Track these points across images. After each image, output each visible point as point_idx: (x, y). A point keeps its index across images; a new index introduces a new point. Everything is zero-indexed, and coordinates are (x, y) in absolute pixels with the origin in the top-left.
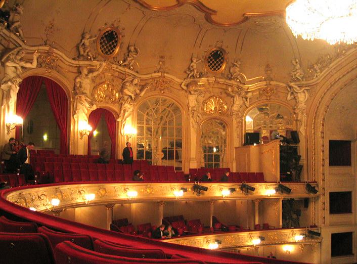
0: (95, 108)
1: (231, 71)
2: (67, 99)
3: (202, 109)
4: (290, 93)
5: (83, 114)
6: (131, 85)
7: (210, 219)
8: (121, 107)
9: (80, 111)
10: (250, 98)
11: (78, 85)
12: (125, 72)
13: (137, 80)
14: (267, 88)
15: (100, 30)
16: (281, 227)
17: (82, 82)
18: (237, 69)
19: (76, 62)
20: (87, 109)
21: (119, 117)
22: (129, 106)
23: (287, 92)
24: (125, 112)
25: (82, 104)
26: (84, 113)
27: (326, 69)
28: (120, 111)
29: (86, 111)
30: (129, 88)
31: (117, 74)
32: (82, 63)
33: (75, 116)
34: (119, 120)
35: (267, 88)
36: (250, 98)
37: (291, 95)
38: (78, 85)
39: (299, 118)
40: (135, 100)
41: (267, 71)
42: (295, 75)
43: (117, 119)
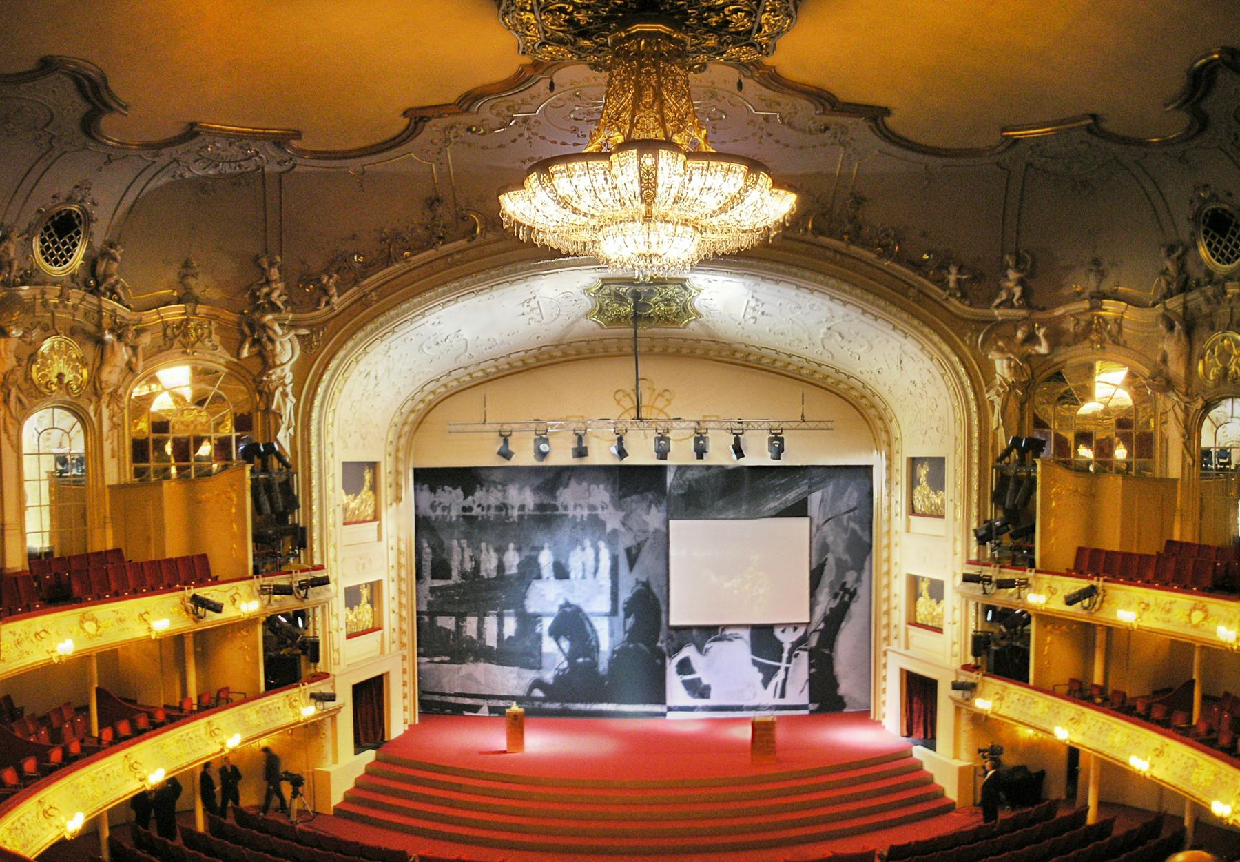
1: (101, 268)
3: (28, 377)
4: (249, 339)
7: (88, 699)
10: (144, 349)
14: (188, 320)
16: (262, 689)
18: (115, 265)
23: (239, 336)
27: (355, 288)
35: (188, 320)
36: (144, 349)
37: (252, 345)
39: (274, 407)
41: (186, 275)
42: (268, 295)
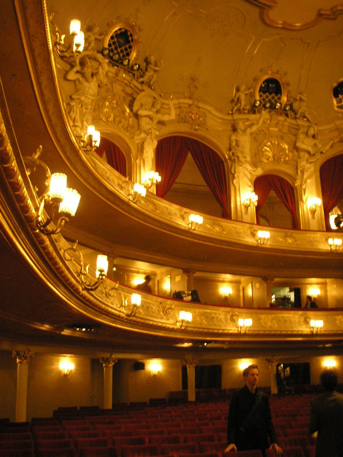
0: (259, 172)
2: (223, 163)
5: (245, 178)
6: (307, 138)
8: (297, 168)
9: (241, 174)
11: (234, 144)
12: (298, 125)
13: (312, 129)
15: (255, 80)
17: (238, 139)
19: (229, 117)
20: (250, 173)
21: (295, 180)
22: (308, 165)
24: (303, 172)
25: (241, 166)
26: (246, 176)
28: (297, 173)
29: (249, 176)
30: (305, 141)
31: (285, 130)
32: (236, 116)
33: (235, 181)
34: (297, 184)
38: (234, 144)
40: (314, 155)
43: (294, 184)
